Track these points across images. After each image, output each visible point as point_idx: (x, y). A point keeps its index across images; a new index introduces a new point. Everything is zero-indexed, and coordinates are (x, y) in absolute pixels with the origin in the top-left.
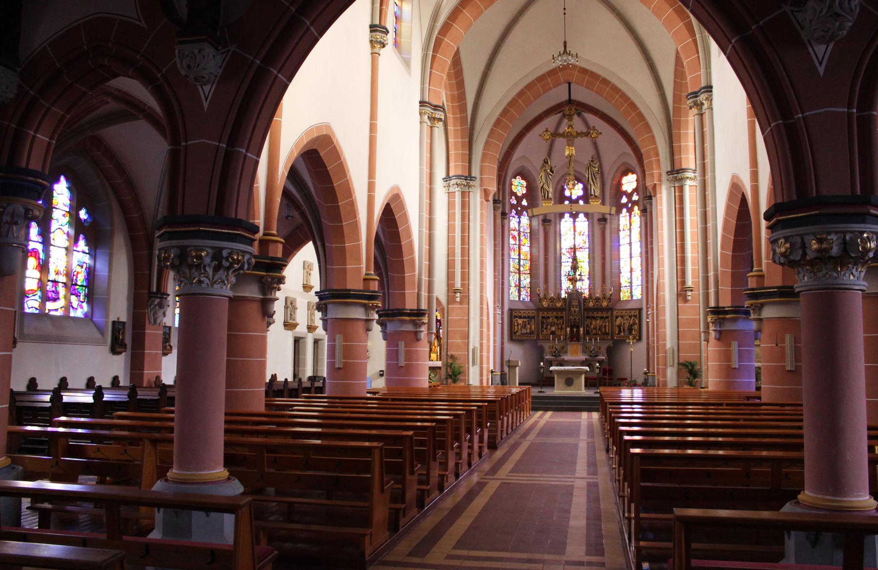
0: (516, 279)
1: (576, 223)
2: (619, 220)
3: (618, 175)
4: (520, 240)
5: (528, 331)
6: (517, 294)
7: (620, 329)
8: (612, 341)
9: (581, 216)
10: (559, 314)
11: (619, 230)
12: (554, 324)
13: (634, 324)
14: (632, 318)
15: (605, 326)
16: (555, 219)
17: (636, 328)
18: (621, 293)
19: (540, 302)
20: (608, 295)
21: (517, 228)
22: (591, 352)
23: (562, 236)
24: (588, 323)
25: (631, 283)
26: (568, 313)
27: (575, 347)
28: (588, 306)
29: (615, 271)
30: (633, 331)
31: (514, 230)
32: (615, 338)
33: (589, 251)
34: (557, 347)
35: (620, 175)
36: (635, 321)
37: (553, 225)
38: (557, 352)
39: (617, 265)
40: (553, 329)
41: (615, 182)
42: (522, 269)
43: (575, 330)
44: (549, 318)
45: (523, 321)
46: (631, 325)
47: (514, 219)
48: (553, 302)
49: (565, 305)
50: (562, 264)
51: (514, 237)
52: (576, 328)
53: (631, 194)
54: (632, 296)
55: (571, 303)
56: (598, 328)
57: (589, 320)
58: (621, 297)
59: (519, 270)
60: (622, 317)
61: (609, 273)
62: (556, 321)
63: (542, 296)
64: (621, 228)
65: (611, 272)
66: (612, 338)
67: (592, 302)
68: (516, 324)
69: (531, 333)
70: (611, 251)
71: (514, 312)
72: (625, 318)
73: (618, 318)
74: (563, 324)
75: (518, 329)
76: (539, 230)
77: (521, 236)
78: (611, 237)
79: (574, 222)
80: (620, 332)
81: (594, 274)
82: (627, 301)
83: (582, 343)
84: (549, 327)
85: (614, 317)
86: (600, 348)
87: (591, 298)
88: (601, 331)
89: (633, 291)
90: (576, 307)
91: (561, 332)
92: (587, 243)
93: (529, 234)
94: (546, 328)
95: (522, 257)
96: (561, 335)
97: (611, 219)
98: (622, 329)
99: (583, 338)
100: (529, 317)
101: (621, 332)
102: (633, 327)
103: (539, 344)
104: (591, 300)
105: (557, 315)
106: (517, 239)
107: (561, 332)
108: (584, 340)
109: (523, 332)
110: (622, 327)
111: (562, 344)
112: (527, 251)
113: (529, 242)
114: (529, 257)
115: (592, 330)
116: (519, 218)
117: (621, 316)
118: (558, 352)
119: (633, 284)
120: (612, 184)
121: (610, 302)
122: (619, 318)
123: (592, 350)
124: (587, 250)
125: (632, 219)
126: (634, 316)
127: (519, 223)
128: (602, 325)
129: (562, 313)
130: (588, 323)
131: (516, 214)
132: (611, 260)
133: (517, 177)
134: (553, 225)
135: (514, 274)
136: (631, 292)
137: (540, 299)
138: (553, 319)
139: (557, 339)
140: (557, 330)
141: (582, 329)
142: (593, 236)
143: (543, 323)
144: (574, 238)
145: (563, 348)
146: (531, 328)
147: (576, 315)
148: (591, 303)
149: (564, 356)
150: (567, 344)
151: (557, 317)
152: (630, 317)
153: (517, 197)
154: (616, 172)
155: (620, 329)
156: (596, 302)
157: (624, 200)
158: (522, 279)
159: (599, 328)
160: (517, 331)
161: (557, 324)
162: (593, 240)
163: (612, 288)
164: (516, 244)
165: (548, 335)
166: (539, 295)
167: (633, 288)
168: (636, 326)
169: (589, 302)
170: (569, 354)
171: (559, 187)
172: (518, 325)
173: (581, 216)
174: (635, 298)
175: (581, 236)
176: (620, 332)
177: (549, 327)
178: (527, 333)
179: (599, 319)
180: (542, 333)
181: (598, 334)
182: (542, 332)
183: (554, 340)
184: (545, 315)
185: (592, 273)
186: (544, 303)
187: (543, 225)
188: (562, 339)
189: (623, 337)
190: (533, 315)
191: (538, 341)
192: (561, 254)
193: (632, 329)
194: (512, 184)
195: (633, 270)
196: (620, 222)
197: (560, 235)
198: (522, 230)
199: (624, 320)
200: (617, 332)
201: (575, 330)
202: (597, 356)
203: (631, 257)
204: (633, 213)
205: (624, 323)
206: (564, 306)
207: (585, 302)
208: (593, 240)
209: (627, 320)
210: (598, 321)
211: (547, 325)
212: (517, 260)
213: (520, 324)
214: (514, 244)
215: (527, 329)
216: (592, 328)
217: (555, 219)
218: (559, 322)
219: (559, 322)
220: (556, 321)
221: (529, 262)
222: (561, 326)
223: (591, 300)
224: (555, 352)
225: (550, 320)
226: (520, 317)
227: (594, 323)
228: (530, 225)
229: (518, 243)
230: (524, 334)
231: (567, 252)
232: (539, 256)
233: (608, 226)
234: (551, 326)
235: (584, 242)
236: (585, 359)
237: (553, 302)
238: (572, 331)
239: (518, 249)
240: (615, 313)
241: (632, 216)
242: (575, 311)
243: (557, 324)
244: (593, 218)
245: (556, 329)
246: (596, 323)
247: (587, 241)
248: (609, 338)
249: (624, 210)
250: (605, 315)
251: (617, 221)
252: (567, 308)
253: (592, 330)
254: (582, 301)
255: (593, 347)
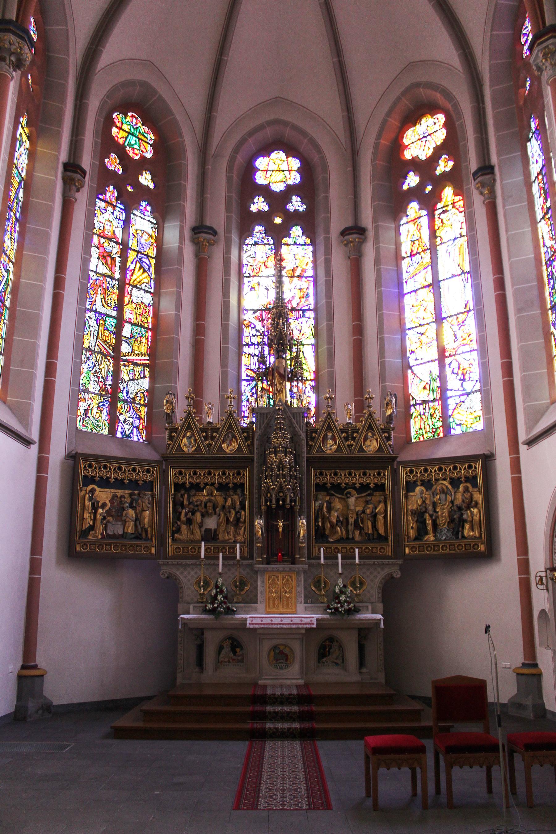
0: (104, 373)
1: (284, 250)
2: (398, 234)
3: (394, 122)
4: (124, 268)
5: (130, 529)
6: (104, 415)
7: (422, 523)
8: (400, 562)
9: (297, 231)
10: (231, 478)
11: (398, 258)
12: (214, 507)
13: (470, 504)
14: (461, 488)
15: (374, 516)
16: (228, 231)
17: (476, 518)
18: (412, 421)
19: (171, 438)
20: (380, 424)
21: (119, 233)
22: (336, 597)
23: (246, 280)
24: (321, 508)
25: (443, 389)
26: (260, 472)
27: (280, 583)
28: (320, 449)
29: (393, 360)
30: (467, 526)
31: (110, 240)
32: (407, 550)
33: (316, 319)
34: (220, 580)
35: (397, 124)
36: (472, 496)
37: (221, 245)
38: (220, 597)
39: (398, 347)
40: (211, 523)
41: (385, 142)
42: (125, 348)
43: (281, 524)
44: (197, 488)
45: (115, 496)
46: (460, 508)
47: (110, 209)
48: (213, 438)
49: (250, 447)
50: (246, 349)
51: (105, 256)
52: (285, 519)
53: (434, 159)
54: (447, 427)
55: (269, 441)
56: (351, 521)
57: (323, 498)
58: (413, 432)
59: (116, 348)
60: (427, 484)
61: (376, 366)
62: (220, 500)
63: (179, 419)
64: (405, 249)
65: (382, 365)
66: (398, 552)
67: (333, 438)
68: (88, 503)
69: (137, 536)
70: (380, 307)
71: (82, 465)
72: (437, 487)
73: (413, 491)
74: (243, 508)
75: (95, 519)
76: (181, 250)
77: (130, 260)
78: (378, 273)
79: (278, 246)
80: (422, 531)
81: (332, 375)
82: (434, 442)
83: (306, 567)
84: (198, 515)
85: (403, 484)
86: (362, 583)
87: (329, 428)
88: (361, 529)
89: (450, 412)
90: (286, 453)
91: (236, 533)
92: (311, 300)
93: (153, 262)
94: (189, 522)
95: (128, 314)
96: (235, 542)
97: (376, 229)
98: (429, 522)
99: (305, 551)
100: (134, 484)
101: (427, 533)
102: (466, 515)
103: (165, 570)
104: (330, 435)
105: (223, 480)
106: (118, 265)
107: (236, 533)
108: (309, 558)
109: (110, 533)
110: (427, 516)
111: (236, 573)
112: (146, 302)
113: (153, 282)
114: (150, 320)
115: (333, 526)
116: (128, 211)
117: (423, 483)
118: (225, 597)
119: (449, 394)
120: (376, 146)
121: (388, 438)
122: (418, 489)
123: (337, 590)
124: (311, 314)
125: (438, 222)
126: (467, 479)
127: (127, 223)
128: (363, 512)
129: (239, 474)
130: (321, 508)
131: (117, 199)
132: (381, 330)
133: (130, 114)
134: (221, 245)
135: (99, 356)
136: (445, 417)
137: (174, 430)
138: (210, 494)
139: (221, 555)
140: (222, 529)
141: (302, 522)
142: (328, 272)
143: (178, 504)
144: (279, 285)
145: (242, 584)
146: (138, 520)
147: (284, 476)
148: (330, 442)
149: (247, 613)
150: (256, 572)
151: (223, 488)
152: (455, 483)
153: (124, 158)
154: (389, 113)
155: (422, 523)
156: (346, 439)
157: (412, 180)
158: (125, 377)
159: (356, 522)
160: (92, 528)
161: (224, 507)
162: (329, 284)
163: (394, 400)
164: (112, 278)
165: (192, 541)
166: (169, 417)
167: (451, 403)
168: (475, 511)
169: (325, 438)
170: (260, 606)
171: (240, 159)
172: (95, 507)
173: (297, 231)
174: (456, 431)
175: (296, 279)
176: (422, 531)
177: (198, 515)
178: (124, 536)
179: (354, 492)
180: (176, 535)
181: (353, 538)
182: (173, 533)
183: (211, 557)
184: (188, 478)
185: (324, 372)
186: (185, 440)
187: (195, 241)
188: (238, 557)
189: (435, 546)
190: (148, 478)
191: (161, 562)
192: (240, 323)
193: (462, 522)
194: (112, 123)
195: (447, 354)
196: (403, 238)
197: (240, 275)
198: (133, 244)
199: (434, 495)
200: (412, 533)
201: (281, 524)
202: (357, 610)
203: (439, 319)
204: (439, 205)
205: (434, 505)
206: (245, 451)
207: (313, 439)
208: (329, 284)
209: (443, 492)
210: (352, 500)
211: (193, 513)
212: (111, 323)
213: (104, 505)
214: (104, 276)
215: (124, 523)
216: (334, 520)
217: (228, 231)
218: (229, 502)
219: (229, 502)
220: (220, 500)
221: (150, 333)
222: (237, 513)
223: (330, 435)
224: (216, 596)
225: (204, 496)
226: (105, 483)
227: (338, 505)
228: (159, 241)
229: (117, 276)
230: (114, 536)
231: (256, 318)
232: (178, 317)
233: (369, 249)
234: (203, 516)
235: (302, 294)
236: (318, 620)
237: (213, 438)
238: (270, 528)
239: (116, 291)
240: (403, 473)
241: (437, 213)
242: (281, 465)
243: (224, 507)
244: (327, 230)
245: (219, 525)
246: (347, 506)
247: (311, 292)
248: (389, 551)
249: (413, 208)
250: (372, 480)
251: (393, 233)
252: (255, 456)
253: (333, 526)
254: (303, 436)
255: (340, 581)
